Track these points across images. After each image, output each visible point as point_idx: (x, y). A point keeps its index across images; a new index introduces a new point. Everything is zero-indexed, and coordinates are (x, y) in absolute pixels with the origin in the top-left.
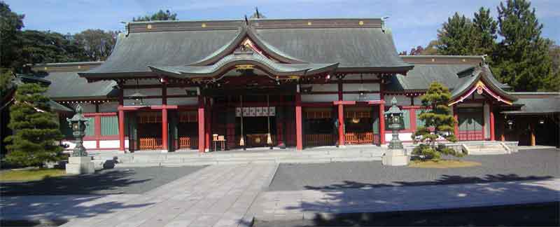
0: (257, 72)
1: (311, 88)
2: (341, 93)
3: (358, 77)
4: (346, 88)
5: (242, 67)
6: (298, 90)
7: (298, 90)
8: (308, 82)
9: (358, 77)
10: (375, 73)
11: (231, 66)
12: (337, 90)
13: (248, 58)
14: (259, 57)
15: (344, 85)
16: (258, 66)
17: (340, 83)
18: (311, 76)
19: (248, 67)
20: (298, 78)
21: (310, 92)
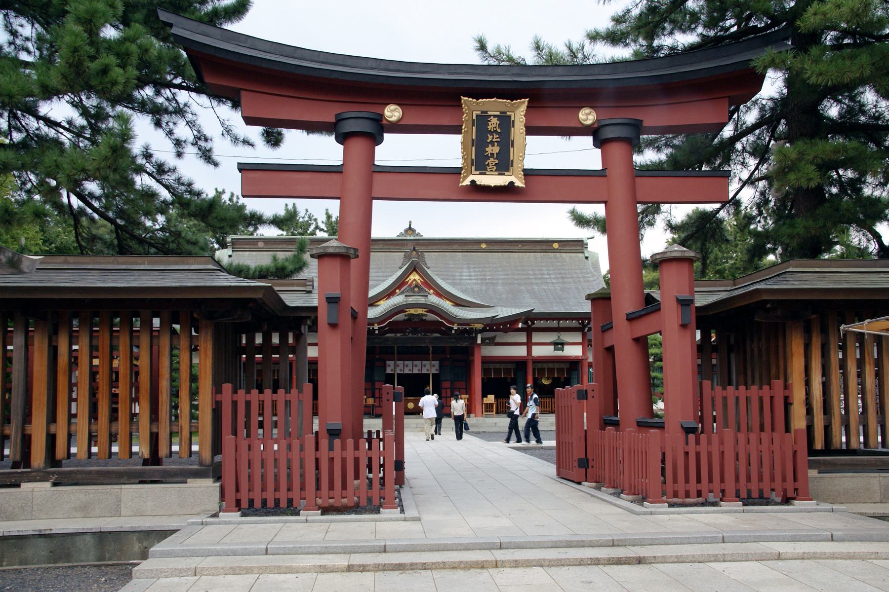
0: (431, 317)
1: (494, 338)
2: (529, 344)
3: (554, 324)
4: (537, 338)
5: (412, 311)
6: (479, 341)
7: (479, 341)
8: (492, 330)
9: (554, 324)
10: (577, 319)
11: (399, 309)
12: (525, 340)
13: (422, 300)
14: (433, 299)
15: (534, 334)
16: (432, 309)
17: (529, 331)
18: (498, 325)
19: (420, 311)
20: (479, 326)
21: (492, 342)
